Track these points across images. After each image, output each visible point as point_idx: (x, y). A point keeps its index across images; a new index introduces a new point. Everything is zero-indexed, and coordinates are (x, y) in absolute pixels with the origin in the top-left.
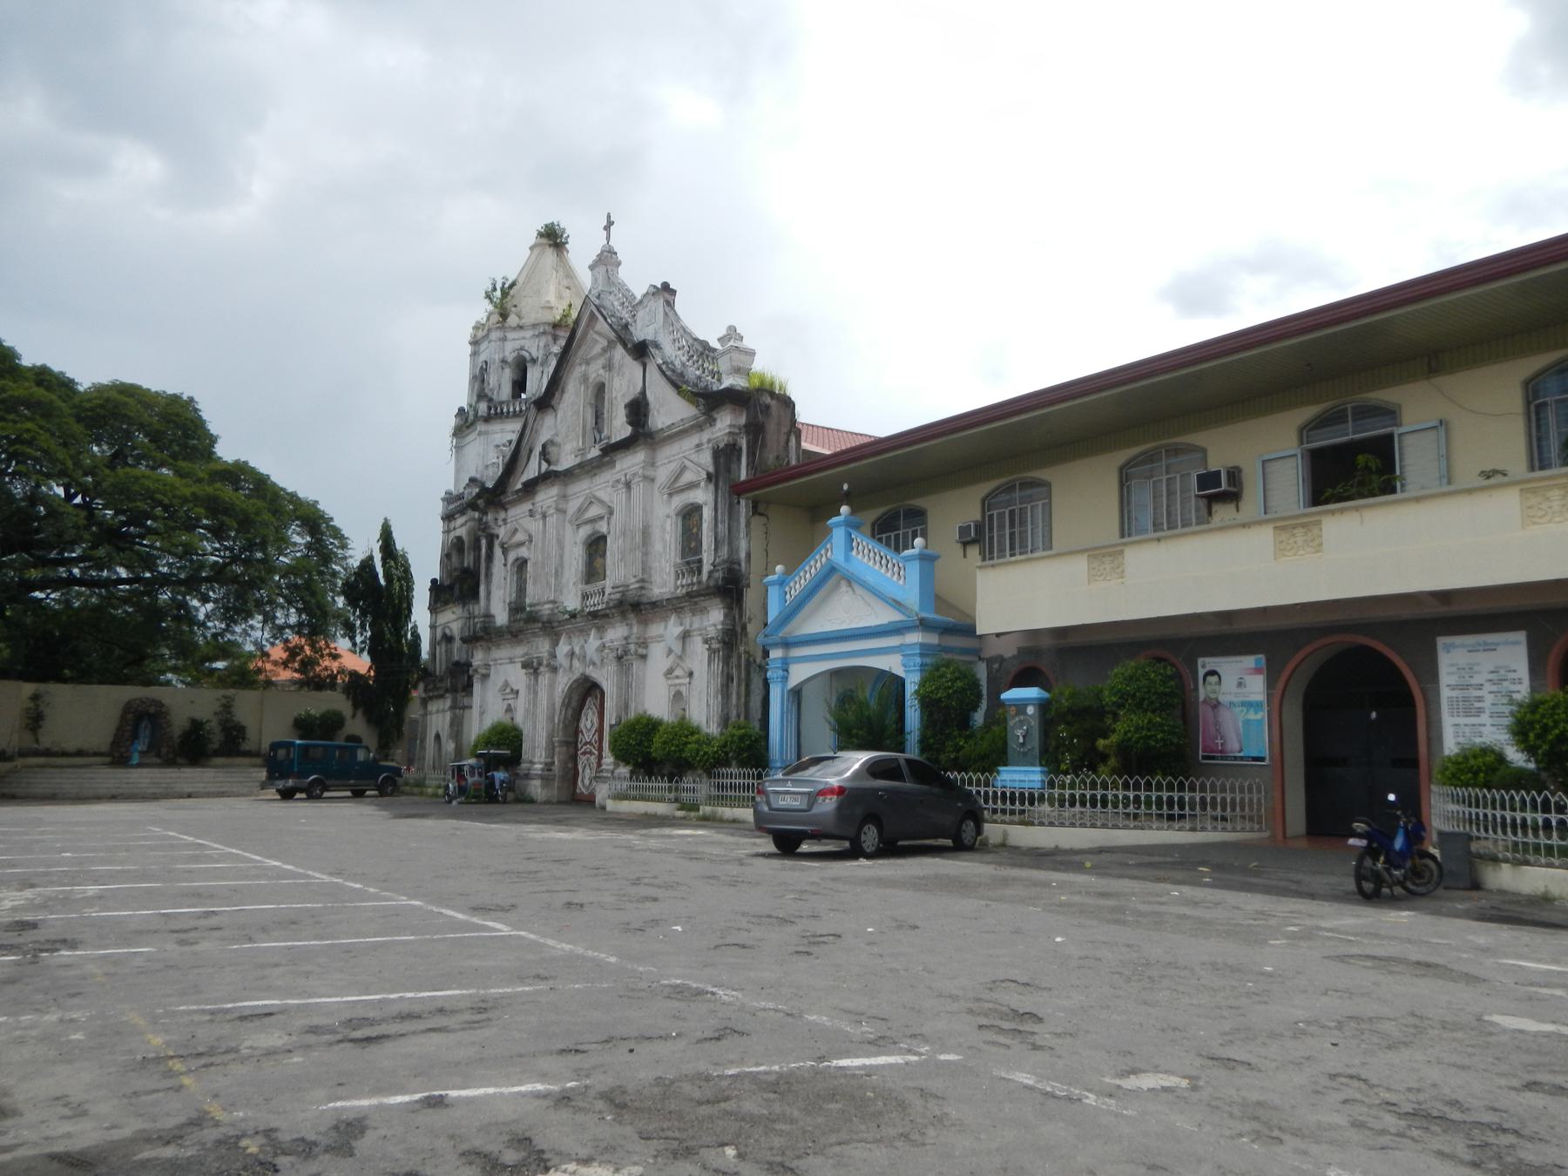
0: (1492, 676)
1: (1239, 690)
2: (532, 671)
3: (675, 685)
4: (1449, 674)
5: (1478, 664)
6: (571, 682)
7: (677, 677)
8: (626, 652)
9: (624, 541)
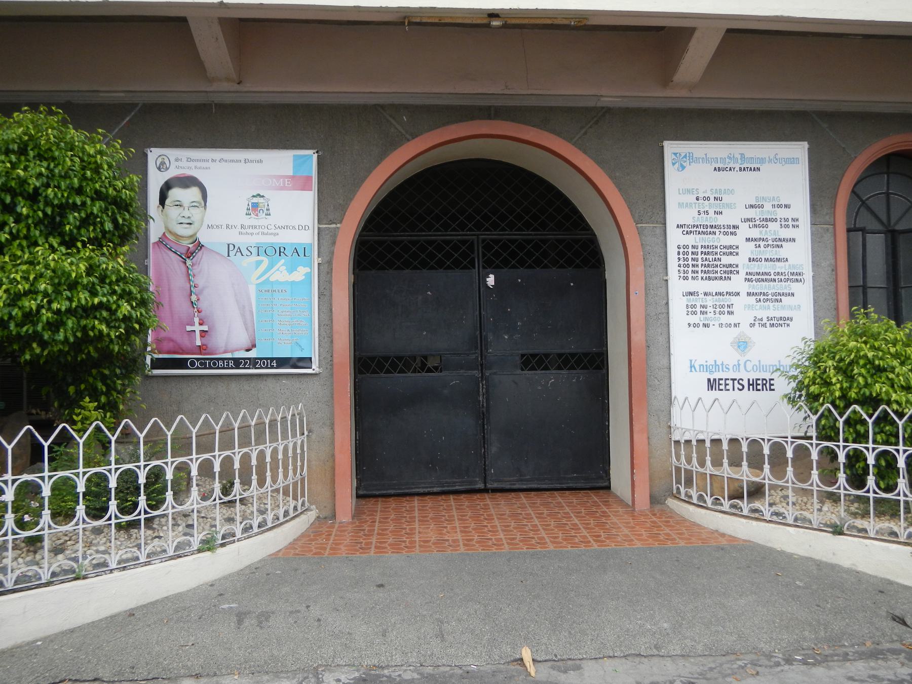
0: (751, 213)
1: (252, 220)
4: (681, 205)
5: (732, 192)
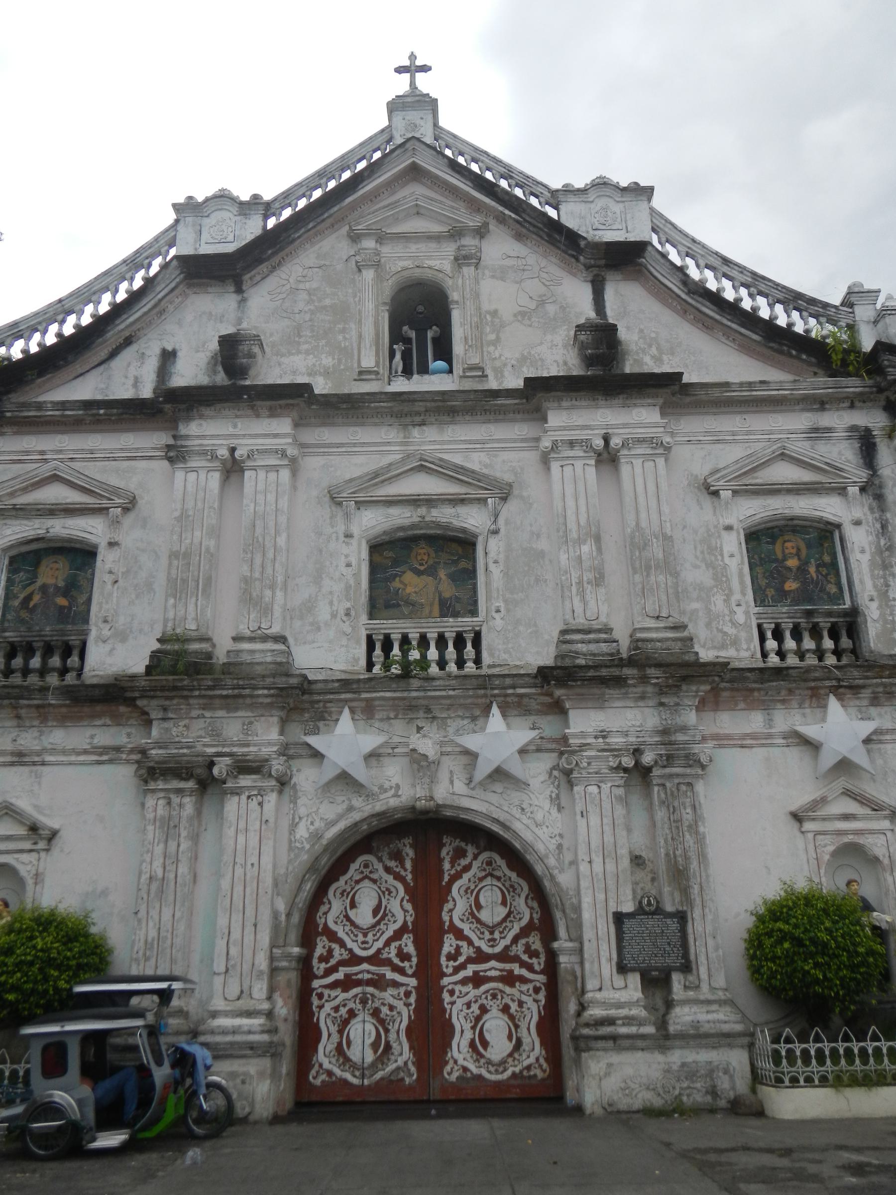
2: (191, 784)
3: (840, 833)
6: (356, 816)
7: (846, 817)
8: (669, 760)
9: (599, 550)
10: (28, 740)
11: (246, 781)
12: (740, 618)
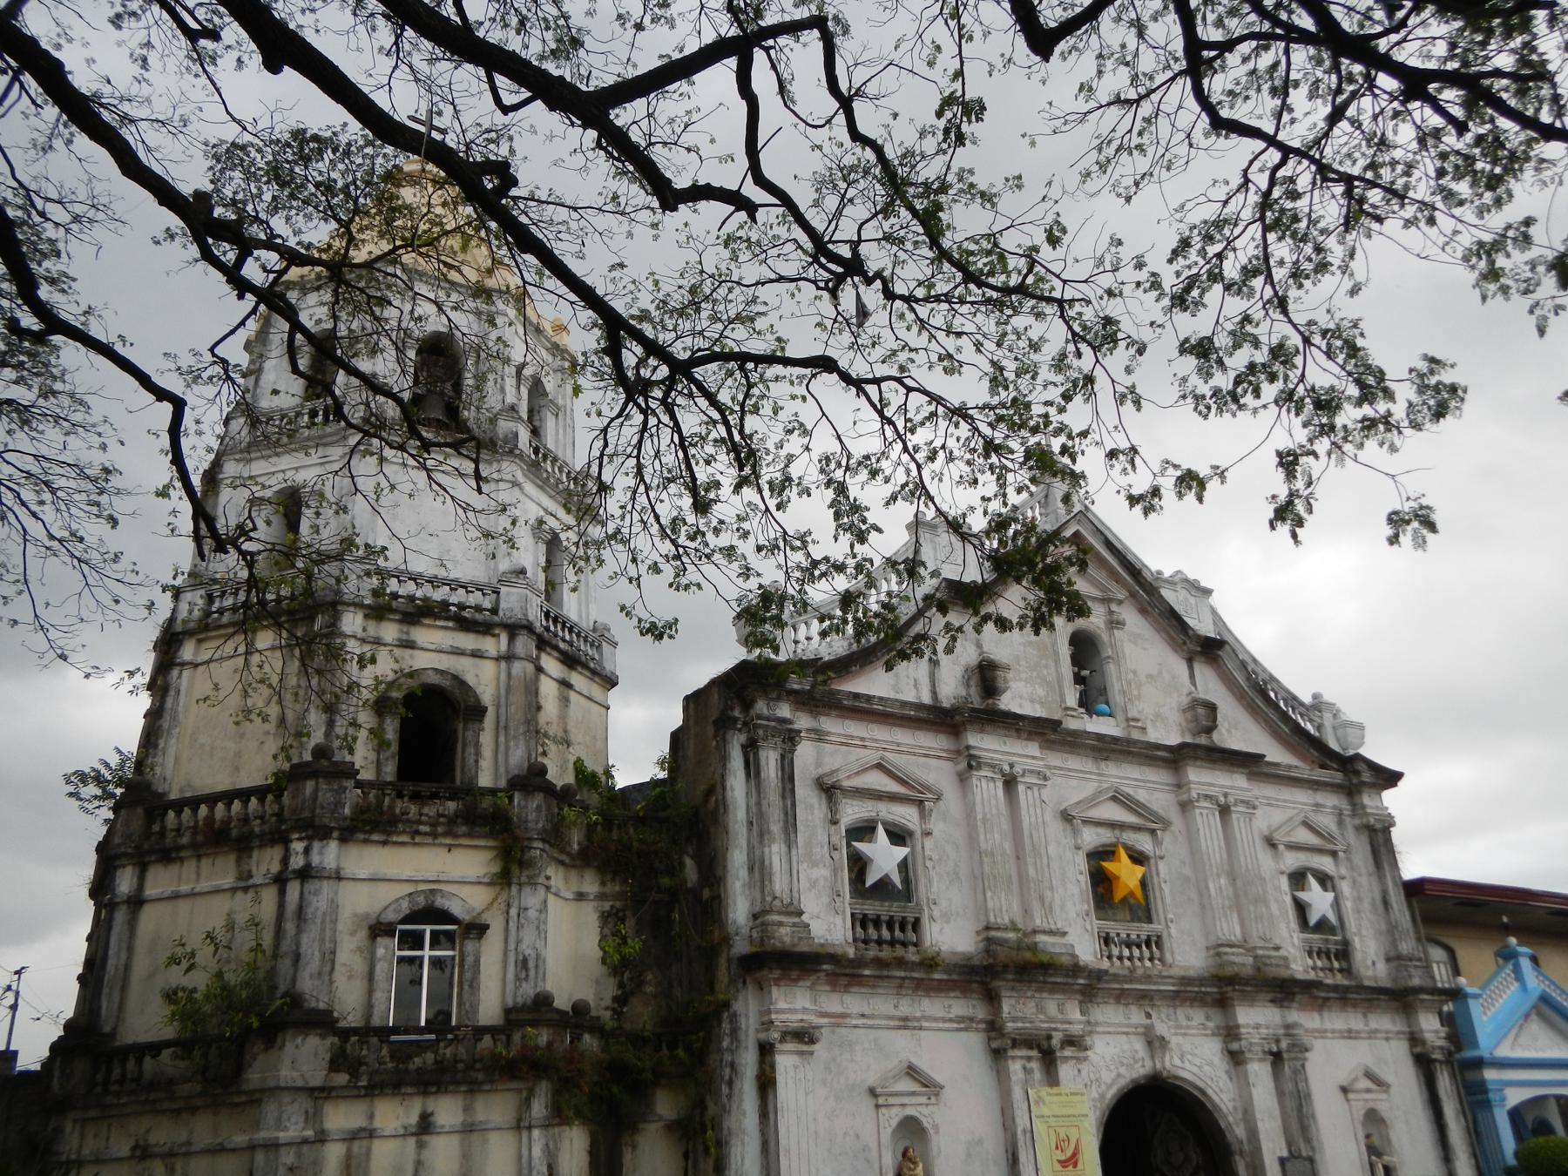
3: (1366, 1100)
10: (907, 1006)
11: (1068, 1052)
12: (1296, 941)
